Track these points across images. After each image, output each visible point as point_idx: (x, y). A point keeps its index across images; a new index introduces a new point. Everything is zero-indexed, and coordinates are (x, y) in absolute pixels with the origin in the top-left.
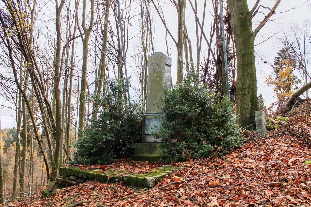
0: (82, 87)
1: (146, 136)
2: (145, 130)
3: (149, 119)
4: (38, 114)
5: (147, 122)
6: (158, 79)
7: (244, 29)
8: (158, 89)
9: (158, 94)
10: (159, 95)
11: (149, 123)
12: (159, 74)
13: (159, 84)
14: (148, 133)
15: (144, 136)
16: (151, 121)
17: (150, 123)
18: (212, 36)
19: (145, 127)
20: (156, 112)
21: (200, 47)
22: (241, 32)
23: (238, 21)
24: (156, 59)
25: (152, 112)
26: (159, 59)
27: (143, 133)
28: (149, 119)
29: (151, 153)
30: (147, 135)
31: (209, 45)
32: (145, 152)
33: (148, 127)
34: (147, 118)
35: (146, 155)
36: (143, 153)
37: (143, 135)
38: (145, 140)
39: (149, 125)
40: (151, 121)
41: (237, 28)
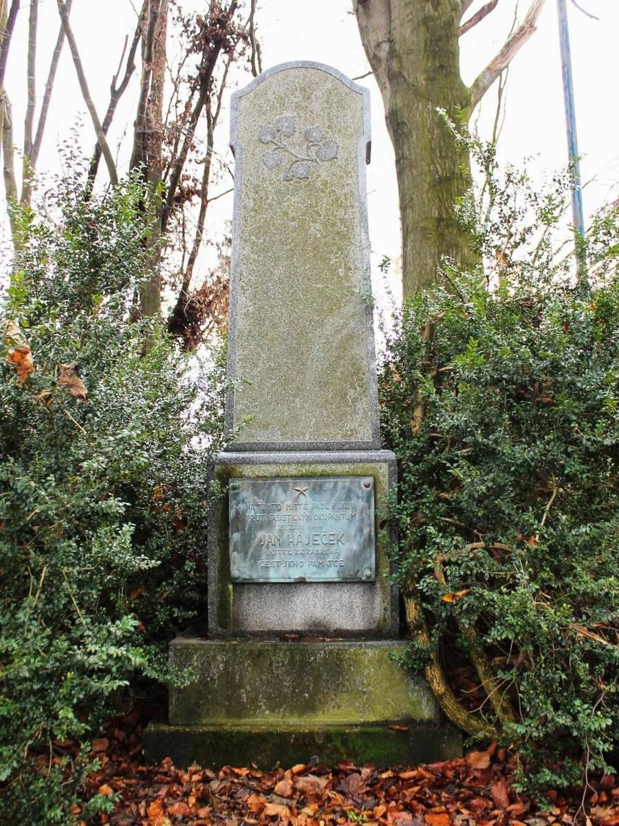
0: (402, 187)
1: (238, 598)
2: (234, 555)
3: (262, 484)
4: (597, 638)
5: (247, 504)
6: (315, 229)
7: (441, 67)
8: (321, 292)
9: (321, 324)
10: (329, 329)
11: (267, 511)
12: (326, 201)
13: (325, 260)
14: (257, 575)
15: (223, 594)
16: (281, 496)
17: (271, 508)
18: (116, 94)
19: (236, 537)
20: (307, 439)
21: (39, 135)
22: (430, 80)
23: (415, 30)
24: (298, 106)
25: (277, 439)
26: (316, 106)
27: (213, 573)
28: (262, 484)
29: (309, 707)
30: (243, 585)
31: (102, 129)
32: (254, 701)
33: (260, 534)
34: (242, 477)
35: (266, 719)
36: (238, 710)
37: (212, 588)
38: (237, 622)
39: (268, 524)
40: (283, 498)
41: (412, 57)
